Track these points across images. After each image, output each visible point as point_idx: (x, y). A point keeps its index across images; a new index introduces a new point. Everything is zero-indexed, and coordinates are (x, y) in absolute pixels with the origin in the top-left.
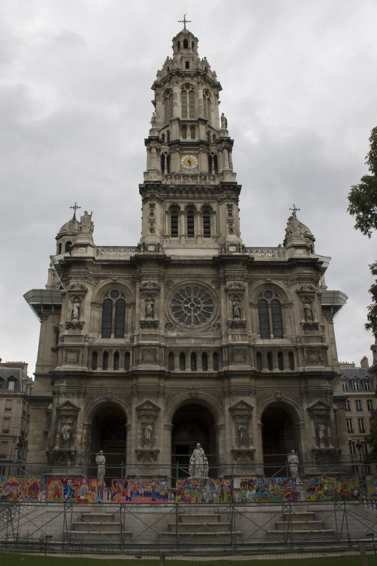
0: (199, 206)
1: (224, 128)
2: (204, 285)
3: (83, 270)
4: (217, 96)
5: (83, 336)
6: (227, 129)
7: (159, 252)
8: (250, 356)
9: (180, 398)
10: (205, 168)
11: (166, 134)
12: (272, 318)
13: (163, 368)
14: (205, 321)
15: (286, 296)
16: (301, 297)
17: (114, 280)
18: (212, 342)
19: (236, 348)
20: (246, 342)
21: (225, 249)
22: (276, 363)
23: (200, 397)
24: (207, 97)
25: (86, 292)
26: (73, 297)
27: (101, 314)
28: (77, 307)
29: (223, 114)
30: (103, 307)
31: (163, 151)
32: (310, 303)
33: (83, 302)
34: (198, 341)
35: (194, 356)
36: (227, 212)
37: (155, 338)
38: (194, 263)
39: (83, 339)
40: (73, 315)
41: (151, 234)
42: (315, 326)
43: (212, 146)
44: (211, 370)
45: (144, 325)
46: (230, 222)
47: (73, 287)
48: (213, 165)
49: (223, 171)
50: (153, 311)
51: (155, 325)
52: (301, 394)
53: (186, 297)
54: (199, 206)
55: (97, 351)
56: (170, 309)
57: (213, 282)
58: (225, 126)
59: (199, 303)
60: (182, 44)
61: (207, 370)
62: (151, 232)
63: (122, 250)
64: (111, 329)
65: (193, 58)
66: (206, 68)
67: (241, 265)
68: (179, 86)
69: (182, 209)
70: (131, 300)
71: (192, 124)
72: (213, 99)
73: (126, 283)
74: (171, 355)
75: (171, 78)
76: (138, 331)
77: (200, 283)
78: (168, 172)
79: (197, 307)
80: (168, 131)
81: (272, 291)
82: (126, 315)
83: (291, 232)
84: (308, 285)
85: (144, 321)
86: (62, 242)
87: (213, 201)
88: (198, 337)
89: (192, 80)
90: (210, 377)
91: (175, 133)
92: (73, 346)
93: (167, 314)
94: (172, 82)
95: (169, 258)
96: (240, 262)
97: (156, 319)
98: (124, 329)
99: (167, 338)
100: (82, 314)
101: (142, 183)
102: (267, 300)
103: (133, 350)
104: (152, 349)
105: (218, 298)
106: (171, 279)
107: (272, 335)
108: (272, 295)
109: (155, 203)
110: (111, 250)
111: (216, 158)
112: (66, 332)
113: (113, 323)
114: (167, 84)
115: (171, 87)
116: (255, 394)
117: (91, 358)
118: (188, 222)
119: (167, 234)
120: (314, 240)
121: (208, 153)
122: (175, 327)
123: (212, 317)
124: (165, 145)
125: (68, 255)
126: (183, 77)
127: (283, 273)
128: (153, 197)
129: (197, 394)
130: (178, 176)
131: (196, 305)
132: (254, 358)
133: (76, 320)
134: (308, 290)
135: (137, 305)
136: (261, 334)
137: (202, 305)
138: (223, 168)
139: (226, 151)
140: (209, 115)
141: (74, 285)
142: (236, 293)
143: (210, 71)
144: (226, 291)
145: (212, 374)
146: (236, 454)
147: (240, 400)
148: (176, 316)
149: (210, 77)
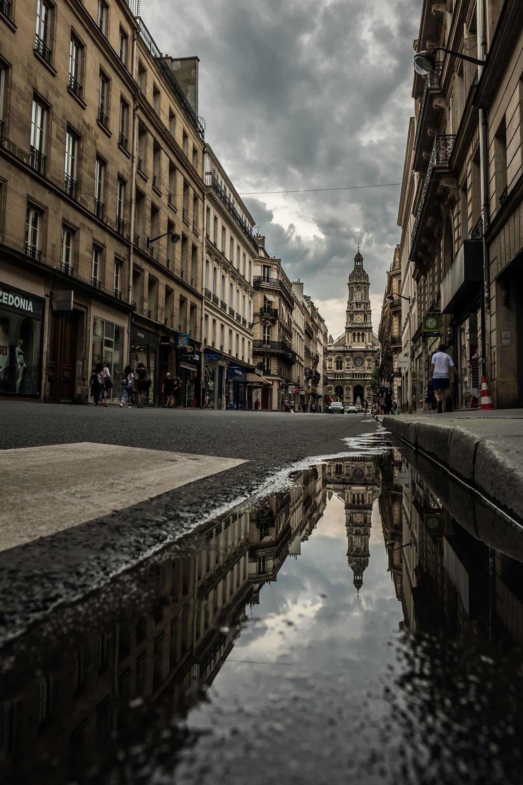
0: (361, 333)
9: (355, 385)
10: (363, 319)
45: (347, 368)
51: (349, 368)
54: (361, 333)
76: (345, 369)
88: (359, 370)
90: (362, 380)
99: (352, 371)
128: (348, 332)
146: (367, 398)
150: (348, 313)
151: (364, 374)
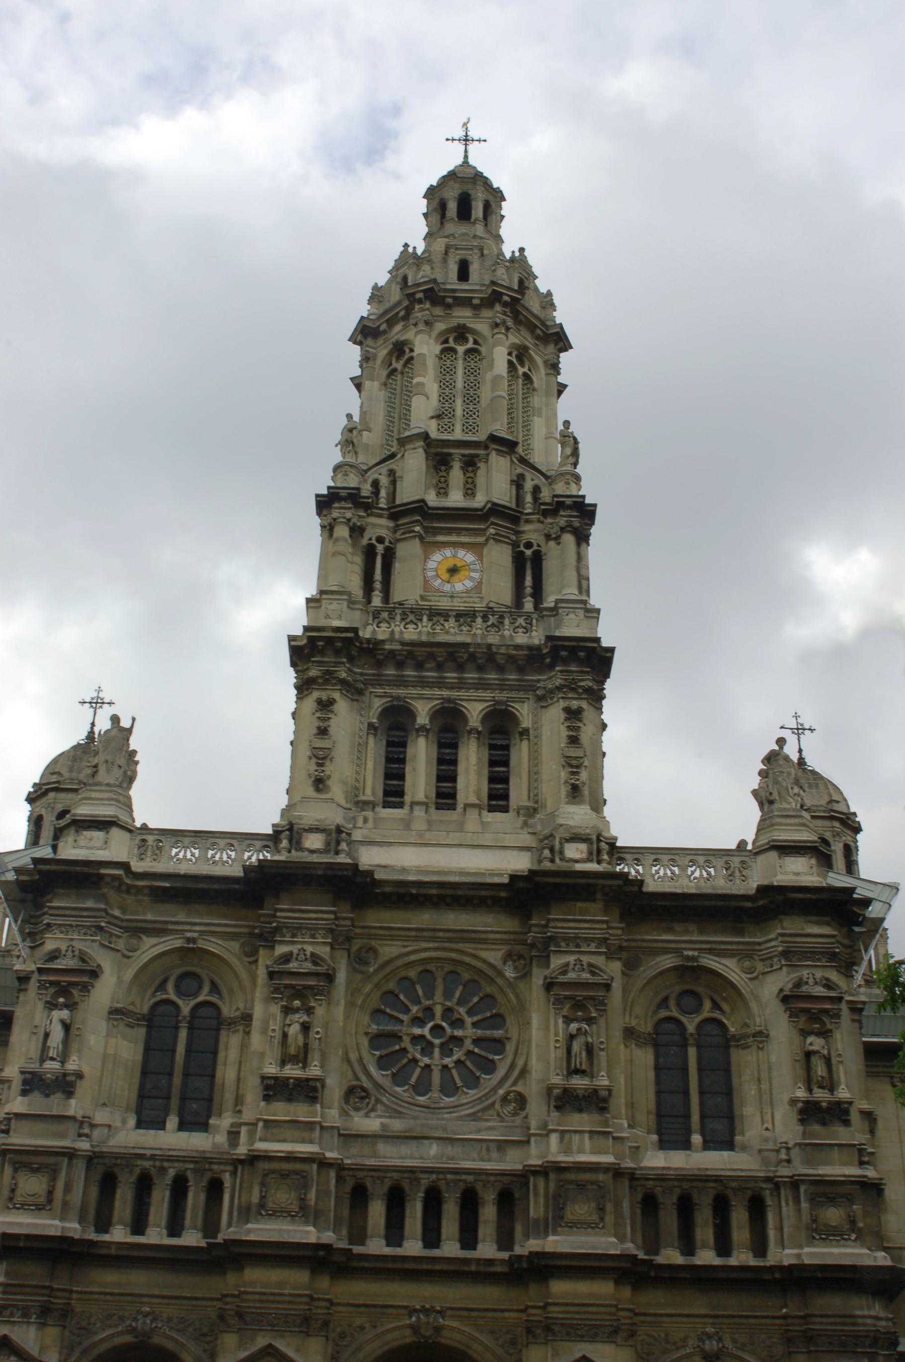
0: (475, 712)
1: (569, 468)
2: (479, 964)
3: (90, 904)
4: (555, 368)
5: (72, 1118)
6: (579, 470)
7: (337, 853)
8: (618, 1205)
10: (500, 588)
11: (384, 481)
12: (696, 1083)
13: (328, 1237)
14: (474, 1082)
15: (747, 1007)
16: (794, 1014)
17: (189, 940)
18: (495, 1155)
19: (572, 1176)
20: (608, 1159)
21: (552, 850)
22: (705, 1232)
23: (448, 1339)
24: (521, 370)
25: (95, 974)
26: (52, 990)
27: (140, 1047)
28: (63, 1022)
29: (567, 424)
30: (150, 1027)
31: (370, 535)
32: (825, 1034)
33: (81, 1006)
34: (450, 1150)
35: (433, 1202)
36: (565, 733)
37: (306, 1134)
38: (449, 892)
39: (73, 1128)
40: (45, 1048)
41: (315, 794)
42: (838, 1113)
43: (528, 521)
44: (487, 1249)
45: (274, 1089)
46: (573, 765)
47: (54, 956)
48: (528, 581)
49: (557, 601)
50: (306, 1045)
51: (308, 1091)
52: (789, 1341)
53: (417, 1001)
54: (475, 712)
55: (117, 1170)
56: (365, 1042)
57: (508, 957)
58: (572, 460)
59: (458, 1023)
60: (452, 207)
61: (474, 1248)
62: (318, 790)
63: (222, 842)
64: (168, 1098)
65: (481, 249)
66: (521, 282)
67: (599, 905)
68: (435, 333)
69: (423, 719)
70: (241, 1006)
71: (467, 452)
72: (540, 378)
73: (228, 950)
74: (359, 1196)
75: (409, 310)
76: (254, 1107)
77: (467, 959)
78: (386, 598)
79: (453, 1038)
80: (392, 473)
81: (700, 989)
82: (221, 1054)
83: (771, 802)
84: (819, 974)
85: (276, 1079)
86: (43, 812)
87: (521, 695)
89: (476, 316)
90: (482, 1274)
91: (414, 480)
92: (37, 1152)
93: (353, 1056)
94: (412, 321)
95: (369, 873)
96: (599, 896)
97: (314, 1071)
98: (210, 1100)
99: (348, 1138)
100: (74, 1046)
101: (299, 632)
102: (684, 1020)
103: (234, 1173)
104: (292, 1171)
105: (522, 1009)
106: (373, 943)
107: (697, 1139)
108: (701, 1005)
109: (336, 695)
110: (187, 841)
111: (538, 559)
112: (19, 1105)
113: (177, 1080)
114: (398, 327)
115: (409, 335)
116: (632, 1335)
117: (94, 1192)
118: (441, 761)
119: (368, 796)
120: (857, 829)
121: (515, 545)
122: (378, 1101)
123: (501, 1072)
124: (380, 516)
125: (45, 852)
126: (449, 307)
127: (740, 932)
128: (328, 678)
129: (438, 1329)
130: (413, 614)
131: (449, 1030)
132: (633, 1214)
133: (55, 1065)
134: (819, 991)
135: (256, 1022)
136: (659, 1132)
137: (468, 1032)
138: (560, 591)
139: (569, 539)
140: (527, 426)
141: (58, 950)
142: (580, 993)
143: (536, 289)
144: (549, 986)
145: (490, 1262)
147: (578, 1355)
148: (383, 1063)
149: (535, 307)
150: (343, 512)
151: (511, 1193)
